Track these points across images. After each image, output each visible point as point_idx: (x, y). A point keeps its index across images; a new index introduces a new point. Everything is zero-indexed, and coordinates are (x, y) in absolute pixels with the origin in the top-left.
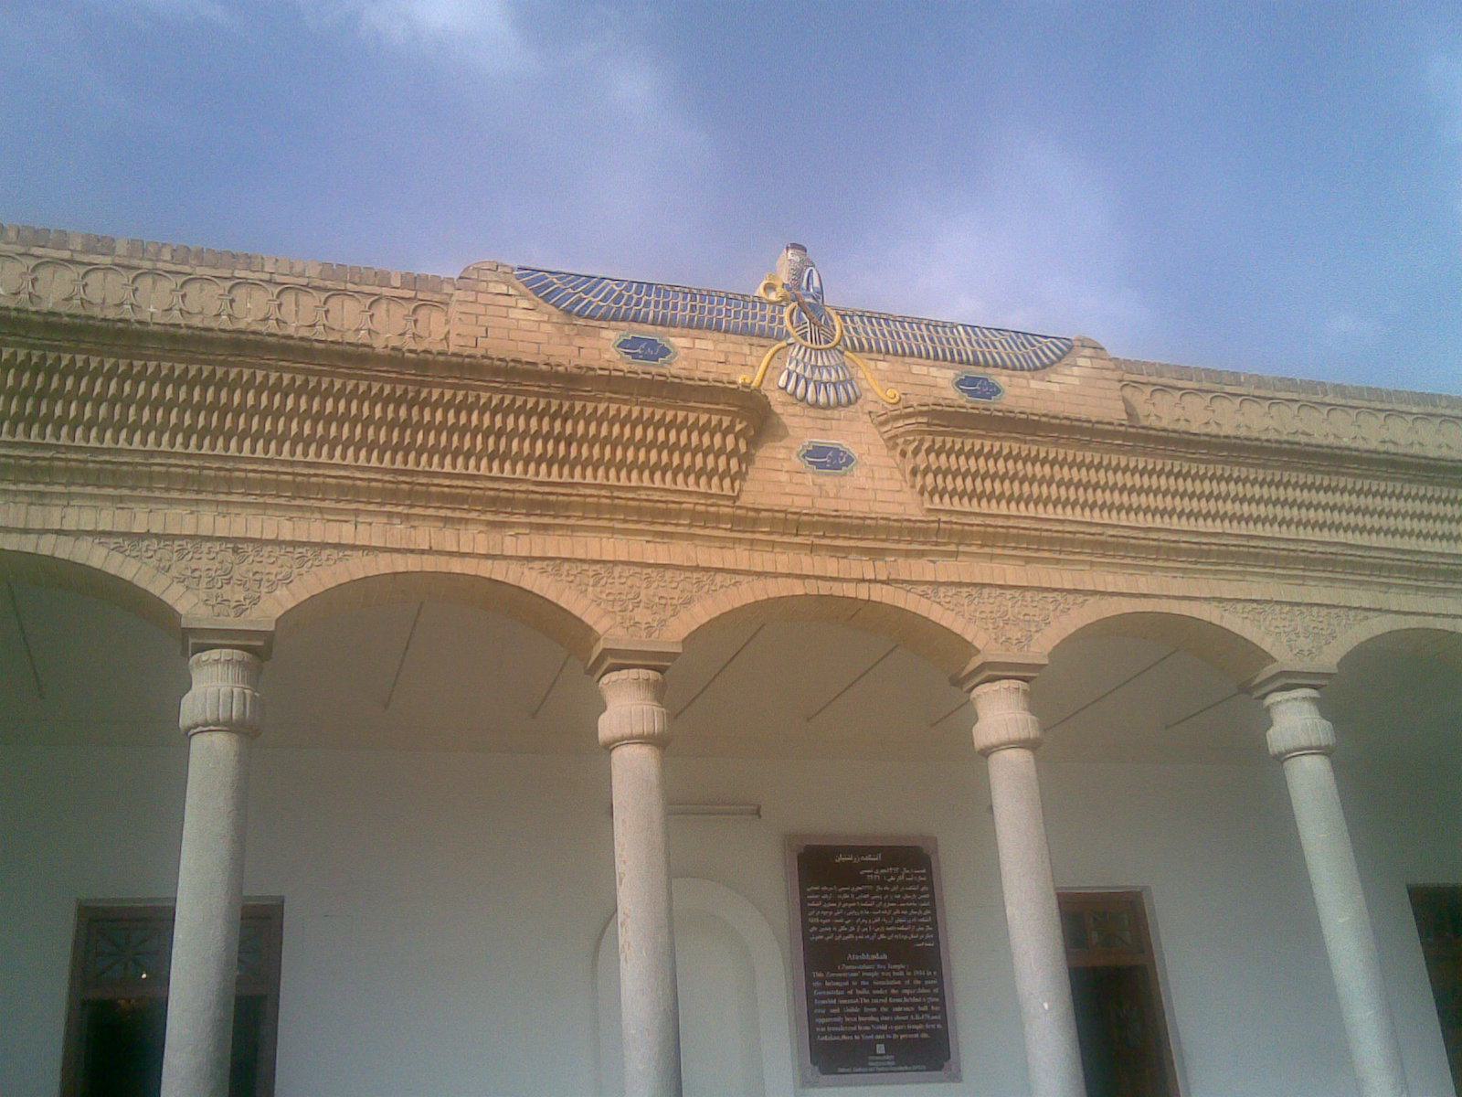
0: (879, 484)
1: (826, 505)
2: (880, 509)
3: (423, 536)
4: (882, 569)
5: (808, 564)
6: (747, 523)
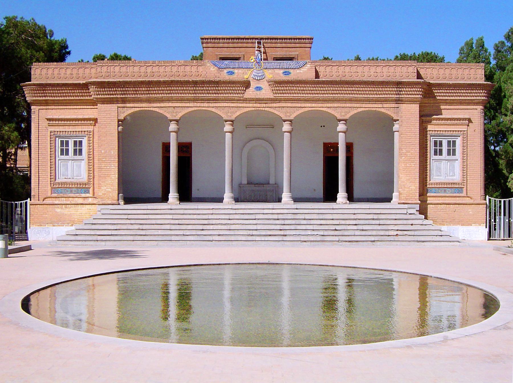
0: (267, 92)
1: (257, 97)
2: (266, 97)
3: (198, 105)
4: (267, 105)
5: (255, 105)
6: (246, 100)
